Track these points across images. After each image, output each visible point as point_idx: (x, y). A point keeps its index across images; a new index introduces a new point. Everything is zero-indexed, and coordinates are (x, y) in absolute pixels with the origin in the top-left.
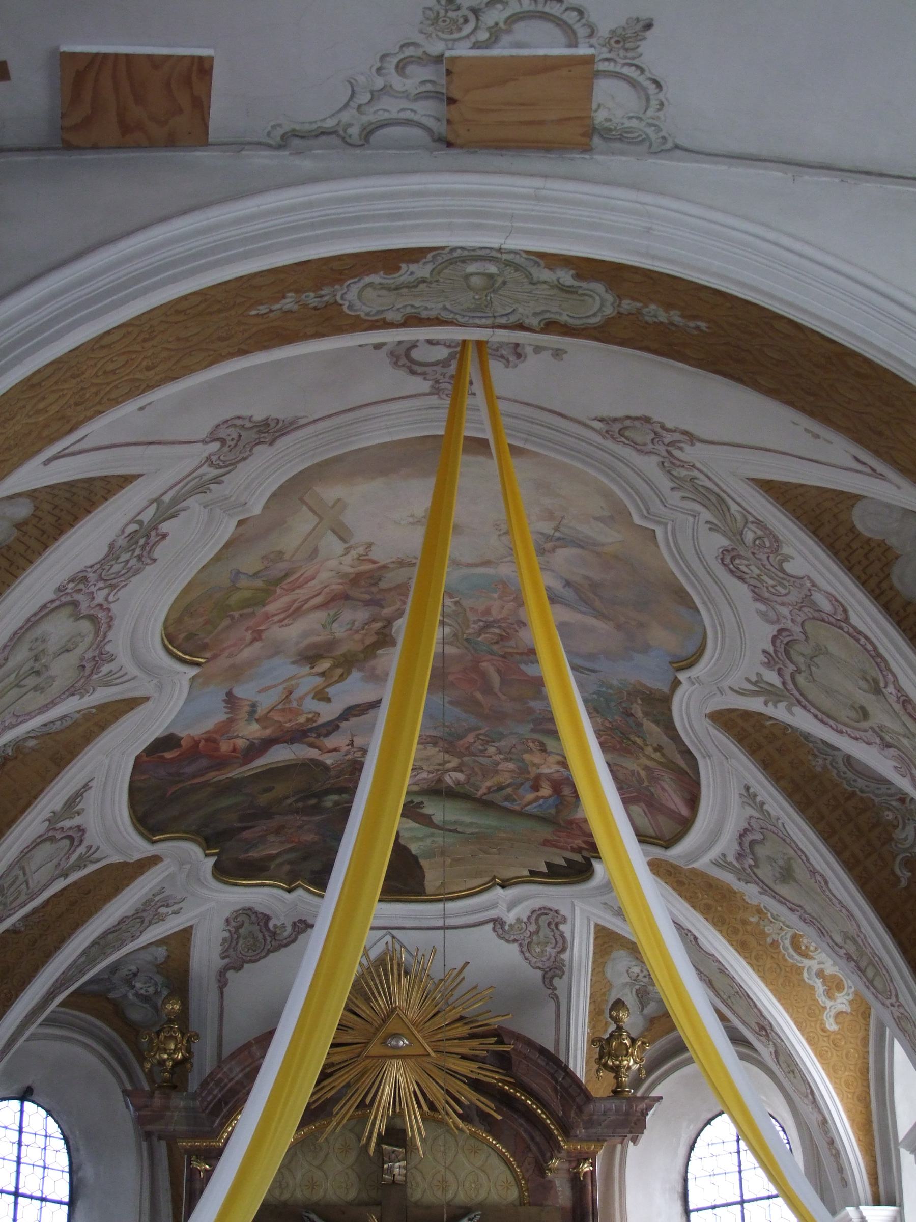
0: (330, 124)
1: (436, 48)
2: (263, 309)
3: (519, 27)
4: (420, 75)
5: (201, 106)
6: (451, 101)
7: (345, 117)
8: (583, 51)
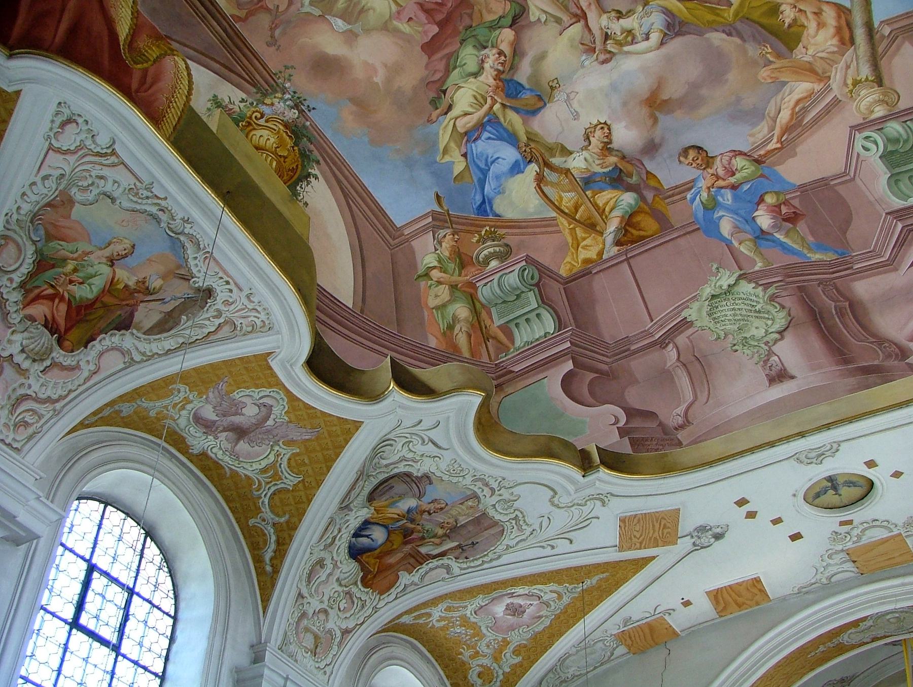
0: (813, 581)
1: (840, 548)
2: (813, 654)
3: (867, 532)
4: (837, 558)
5: (763, 591)
6: (854, 562)
7: (818, 577)
8: (896, 532)
